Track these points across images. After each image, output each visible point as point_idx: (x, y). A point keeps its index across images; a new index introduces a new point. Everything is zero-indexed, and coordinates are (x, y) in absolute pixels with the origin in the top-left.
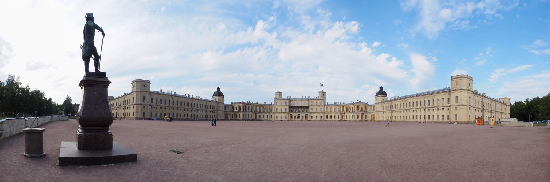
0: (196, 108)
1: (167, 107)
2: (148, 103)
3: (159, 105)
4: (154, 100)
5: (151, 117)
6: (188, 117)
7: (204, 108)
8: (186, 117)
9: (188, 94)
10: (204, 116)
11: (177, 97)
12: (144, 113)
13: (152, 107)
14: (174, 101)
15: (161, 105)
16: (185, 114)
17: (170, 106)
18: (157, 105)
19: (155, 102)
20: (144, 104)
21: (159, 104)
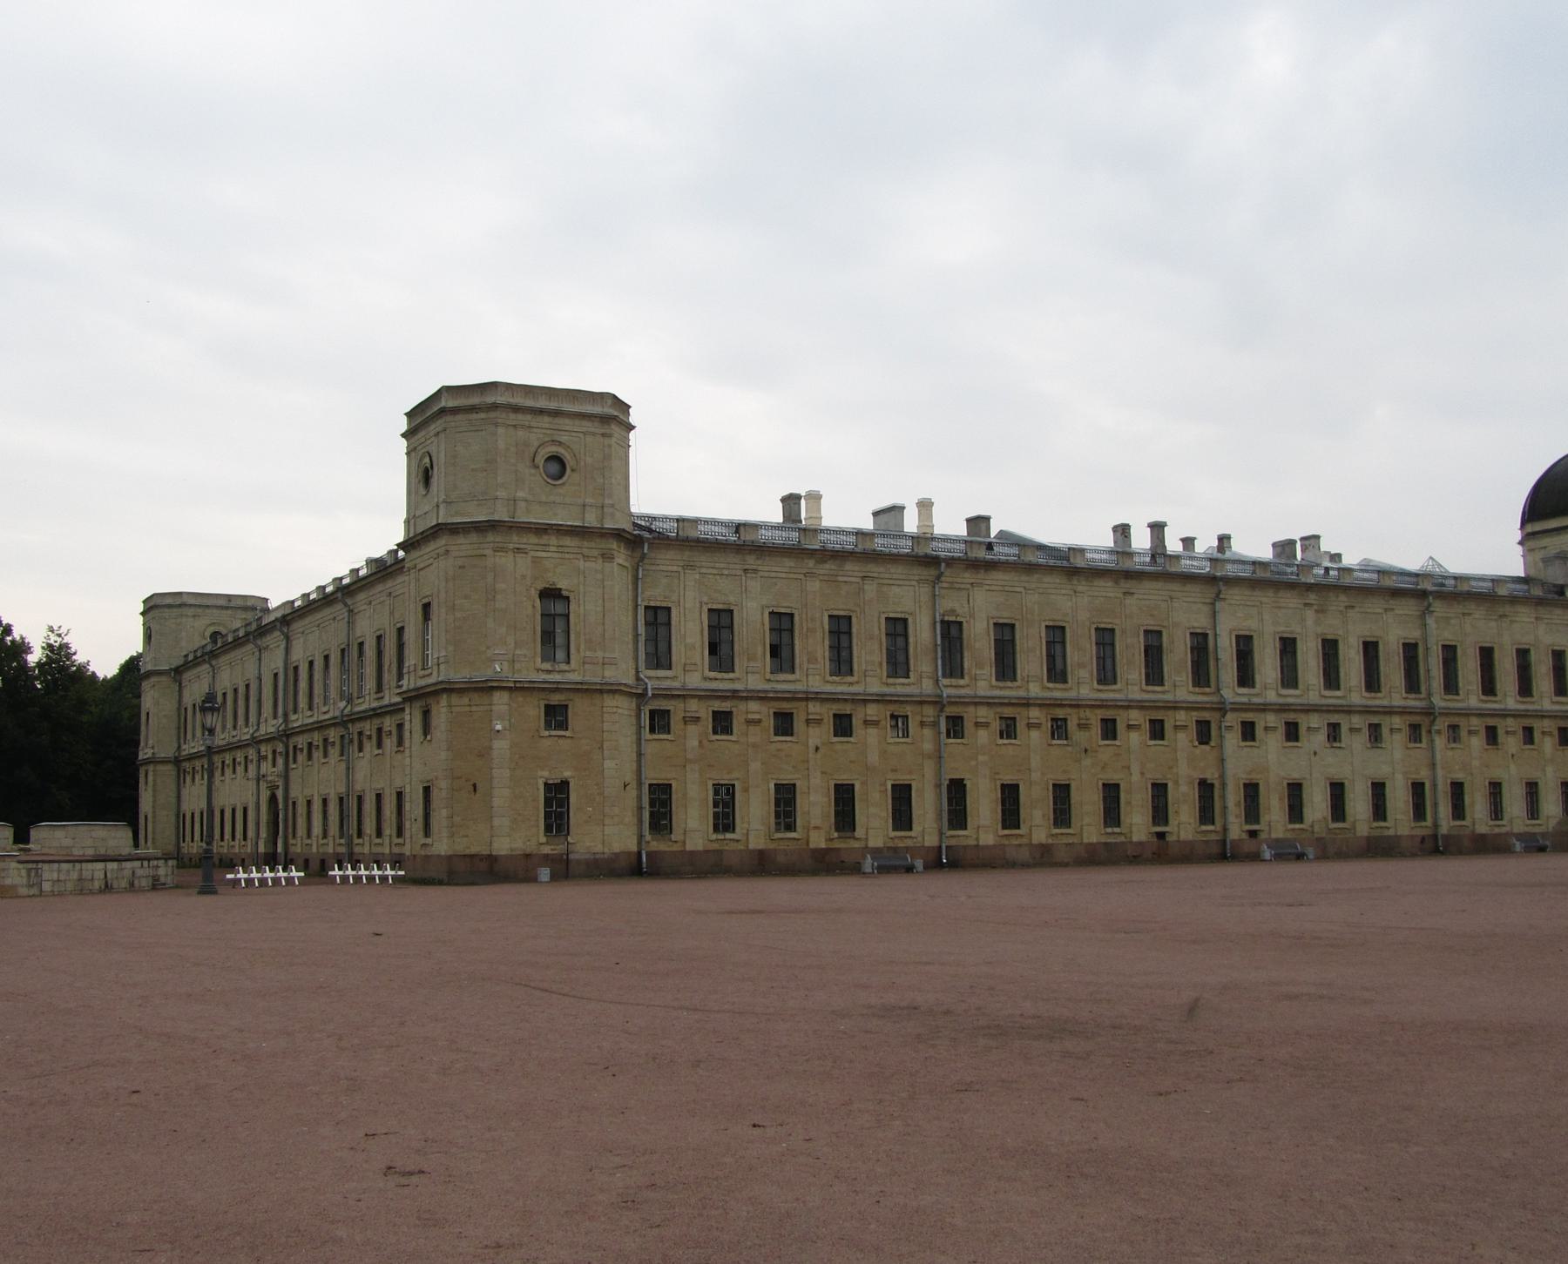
0: (1272, 697)
1: (872, 711)
2: (611, 675)
3: (755, 683)
4: (689, 634)
5: (656, 845)
6: (1160, 812)
7: (1394, 691)
8: (1137, 822)
9: (1157, 528)
10: (1399, 800)
11: (998, 577)
12: (557, 794)
13: (660, 721)
14: (951, 635)
15: (785, 683)
16: (1112, 777)
17: (900, 687)
18: (723, 682)
19: (702, 656)
20: (556, 688)
21: (753, 671)
